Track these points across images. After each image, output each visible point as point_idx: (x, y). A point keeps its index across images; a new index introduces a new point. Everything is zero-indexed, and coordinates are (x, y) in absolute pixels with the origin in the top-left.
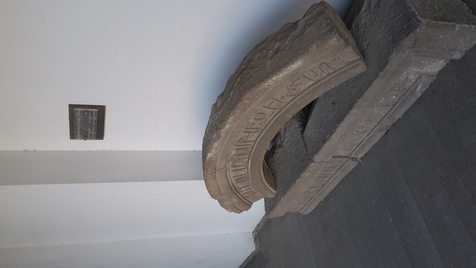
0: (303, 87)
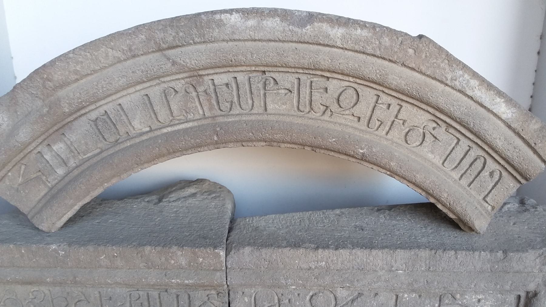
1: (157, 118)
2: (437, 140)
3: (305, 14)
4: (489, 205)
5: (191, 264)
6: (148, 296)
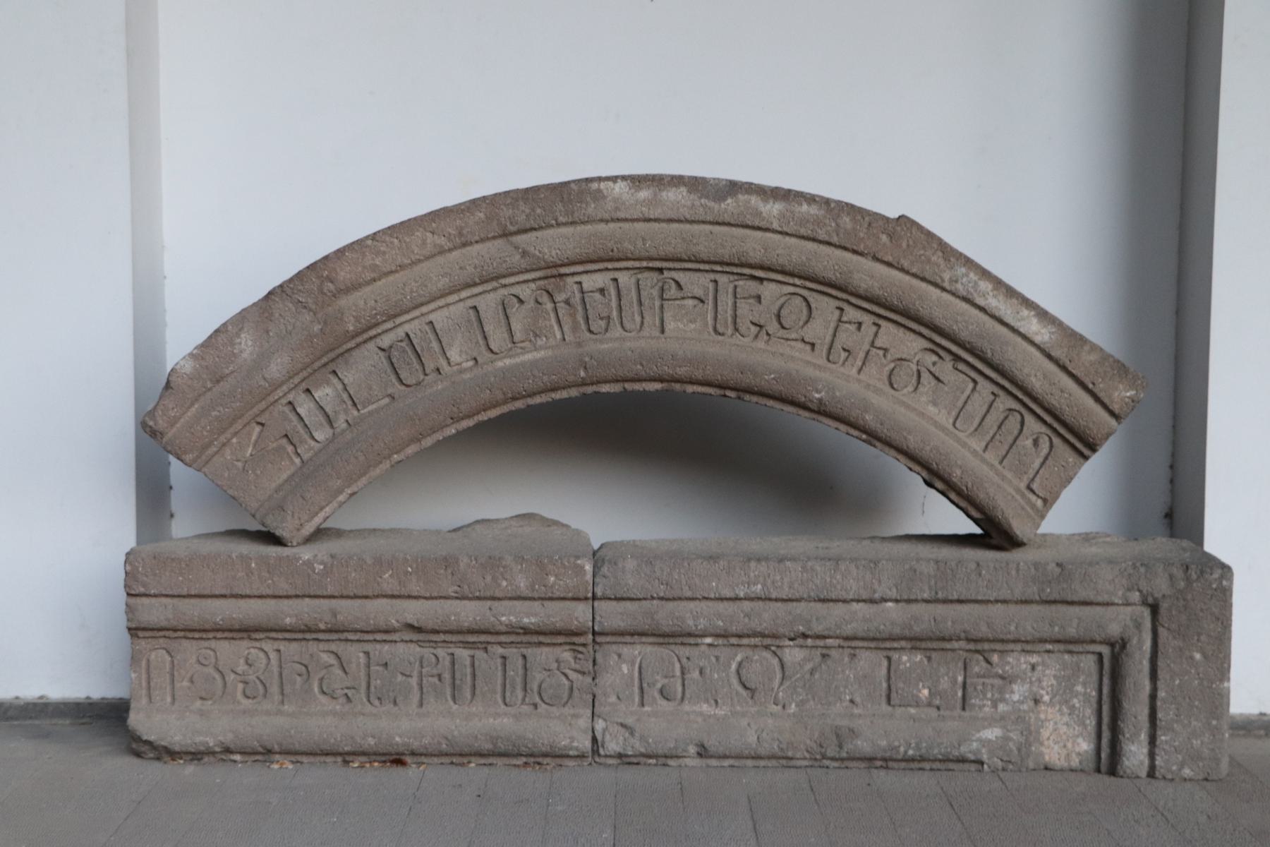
1: (488, 345)
2: (940, 384)
3: (724, 183)
4: (1038, 496)
5: (534, 586)
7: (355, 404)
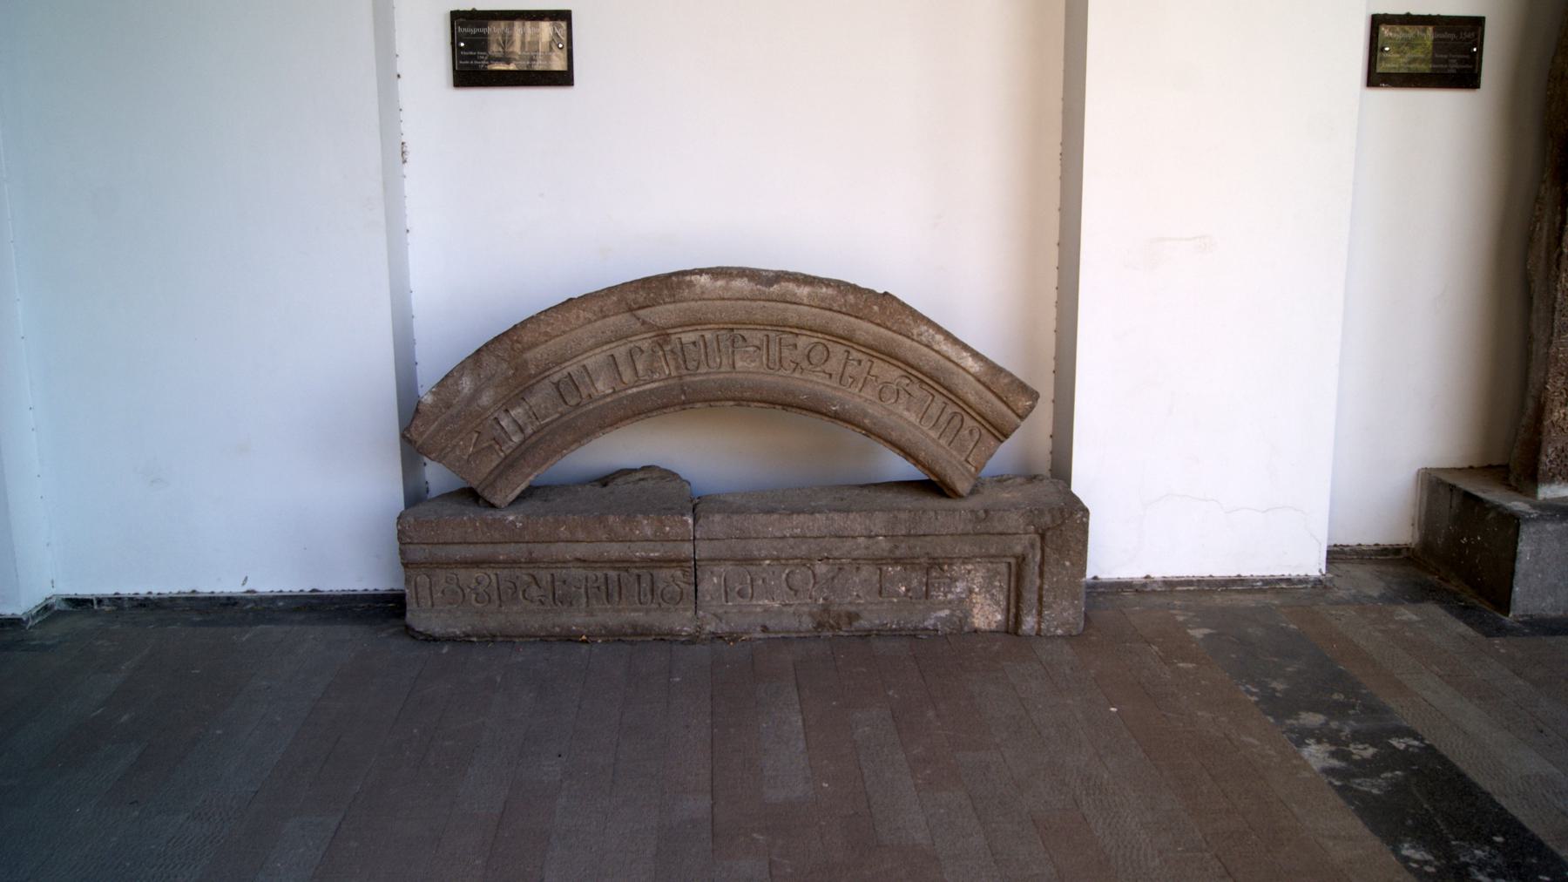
0: (900, 409)
1: (621, 379)
3: (772, 274)
6: (606, 579)
7: (537, 418)
